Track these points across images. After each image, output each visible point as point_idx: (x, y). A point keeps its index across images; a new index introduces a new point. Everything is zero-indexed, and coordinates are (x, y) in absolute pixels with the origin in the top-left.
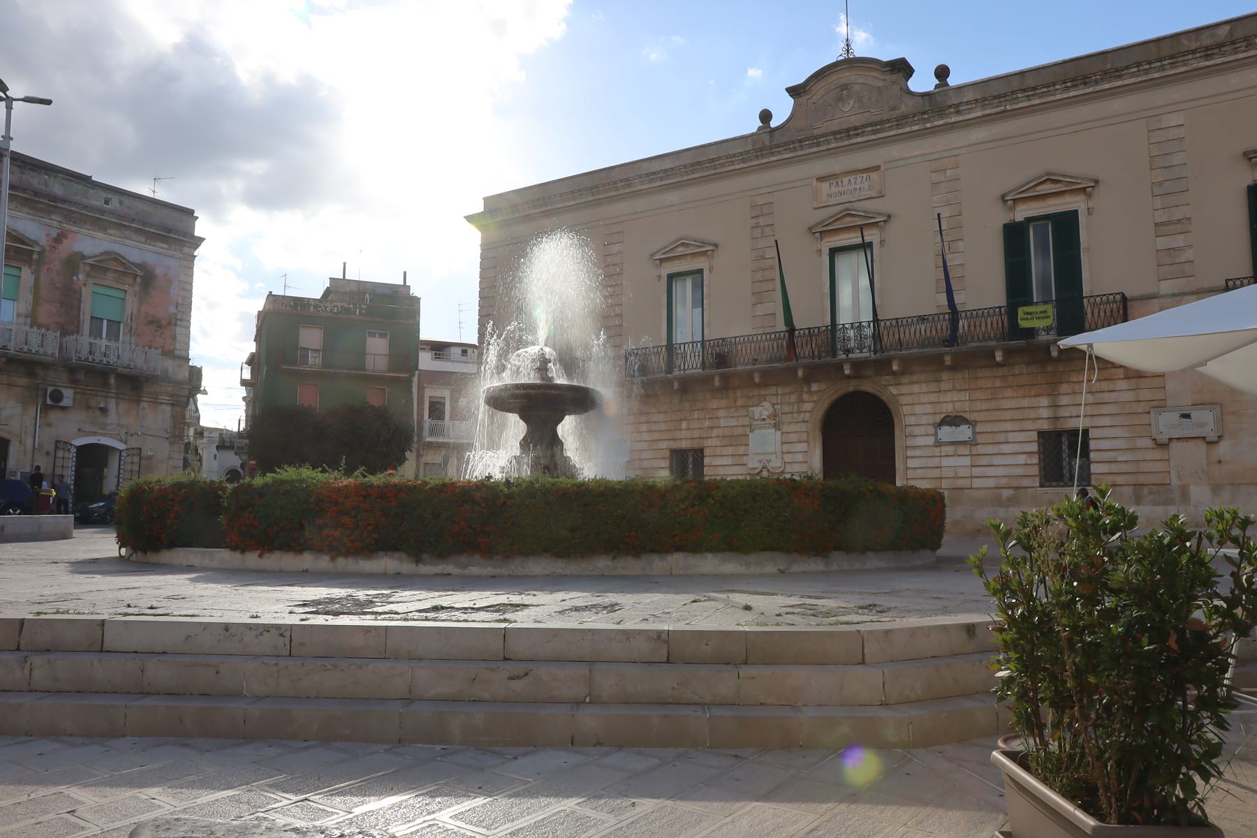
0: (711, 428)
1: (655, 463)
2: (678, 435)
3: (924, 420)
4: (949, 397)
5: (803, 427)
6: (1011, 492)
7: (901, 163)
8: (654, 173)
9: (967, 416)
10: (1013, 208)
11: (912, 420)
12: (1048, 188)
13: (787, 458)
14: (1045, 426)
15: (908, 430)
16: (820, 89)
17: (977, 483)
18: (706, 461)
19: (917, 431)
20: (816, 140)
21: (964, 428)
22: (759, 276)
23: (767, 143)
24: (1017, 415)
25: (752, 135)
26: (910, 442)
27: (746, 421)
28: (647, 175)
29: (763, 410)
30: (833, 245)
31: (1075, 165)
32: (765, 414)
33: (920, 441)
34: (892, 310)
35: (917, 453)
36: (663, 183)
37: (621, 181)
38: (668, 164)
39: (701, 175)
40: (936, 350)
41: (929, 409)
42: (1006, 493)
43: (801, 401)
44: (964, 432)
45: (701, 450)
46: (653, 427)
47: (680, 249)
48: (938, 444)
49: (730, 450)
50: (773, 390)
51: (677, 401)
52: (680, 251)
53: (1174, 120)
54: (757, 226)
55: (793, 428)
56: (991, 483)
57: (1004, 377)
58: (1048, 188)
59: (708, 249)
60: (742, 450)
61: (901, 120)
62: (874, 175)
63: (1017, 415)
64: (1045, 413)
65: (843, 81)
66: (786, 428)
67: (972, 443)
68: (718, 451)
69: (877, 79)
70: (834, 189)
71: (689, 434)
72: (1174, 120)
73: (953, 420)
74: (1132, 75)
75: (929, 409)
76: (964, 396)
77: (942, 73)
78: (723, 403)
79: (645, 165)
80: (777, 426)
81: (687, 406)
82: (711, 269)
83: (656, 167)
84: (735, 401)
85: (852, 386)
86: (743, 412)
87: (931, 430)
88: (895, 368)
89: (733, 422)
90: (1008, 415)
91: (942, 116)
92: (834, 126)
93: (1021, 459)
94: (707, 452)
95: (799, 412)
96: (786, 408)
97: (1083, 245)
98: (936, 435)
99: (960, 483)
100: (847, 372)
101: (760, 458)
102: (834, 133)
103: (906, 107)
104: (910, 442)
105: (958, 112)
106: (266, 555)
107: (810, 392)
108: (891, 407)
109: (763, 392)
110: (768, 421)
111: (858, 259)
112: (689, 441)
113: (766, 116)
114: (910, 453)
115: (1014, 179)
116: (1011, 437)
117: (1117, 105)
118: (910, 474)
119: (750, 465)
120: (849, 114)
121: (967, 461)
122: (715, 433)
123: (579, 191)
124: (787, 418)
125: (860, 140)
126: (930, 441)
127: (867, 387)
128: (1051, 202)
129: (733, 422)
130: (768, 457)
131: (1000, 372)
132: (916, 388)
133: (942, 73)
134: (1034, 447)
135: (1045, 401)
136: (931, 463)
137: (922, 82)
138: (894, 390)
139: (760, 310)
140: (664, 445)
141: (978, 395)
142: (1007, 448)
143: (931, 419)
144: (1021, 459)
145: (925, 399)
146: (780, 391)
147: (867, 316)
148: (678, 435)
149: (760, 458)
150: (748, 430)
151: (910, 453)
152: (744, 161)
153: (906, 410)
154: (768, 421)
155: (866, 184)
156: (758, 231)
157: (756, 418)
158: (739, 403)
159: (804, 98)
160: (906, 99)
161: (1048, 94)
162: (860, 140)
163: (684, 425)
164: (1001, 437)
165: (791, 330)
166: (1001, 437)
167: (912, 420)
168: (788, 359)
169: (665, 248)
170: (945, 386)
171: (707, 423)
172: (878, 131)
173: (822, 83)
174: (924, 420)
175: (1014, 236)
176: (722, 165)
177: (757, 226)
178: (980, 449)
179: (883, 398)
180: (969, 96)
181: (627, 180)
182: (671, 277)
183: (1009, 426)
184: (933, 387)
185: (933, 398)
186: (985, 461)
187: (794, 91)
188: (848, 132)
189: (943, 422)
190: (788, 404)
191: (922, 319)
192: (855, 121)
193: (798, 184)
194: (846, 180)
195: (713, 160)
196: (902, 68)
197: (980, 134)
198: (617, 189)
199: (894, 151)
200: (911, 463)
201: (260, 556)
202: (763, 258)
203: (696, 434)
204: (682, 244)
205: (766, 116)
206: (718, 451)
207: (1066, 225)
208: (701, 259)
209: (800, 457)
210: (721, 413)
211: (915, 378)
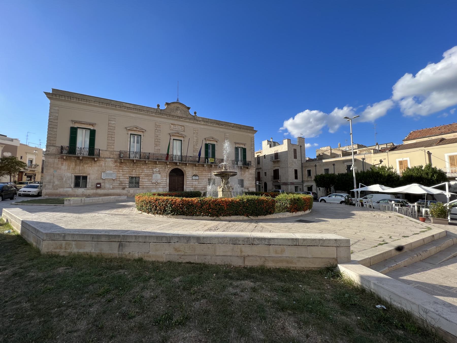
0: (142, 172)
1: (124, 180)
2: (132, 173)
3: (190, 175)
4: (195, 171)
5: (166, 174)
6: (204, 188)
7: (188, 127)
8: (130, 108)
9: (198, 175)
10: (206, 141)
11: (188, 175)
12: (211, 139)
13: (162, 180)
14: (209, 178)
15: (187, 177)
16: (173, 105)
17: (199, 187)
18: (140, 180)
19: (189, 177)
20: (173, 116)
21: (197, 177)
22: (156, 140)
23: (160, 112)
24: (205, 175)
25: (156, 109)
26: (187, 179)
27: (152, 172)
28: (127, 107)
29: (157, 169)
30: (174, 138)
31: (215, 137)
32: (157, 171)
33: (189, 179)
34: (184, 154)
35: (189, 181)
36: (131, 111)
37: (118, 106)
38: (131, 106)
39: (143, 113)
40: (196, 163)
41: (191, 173)
42: (203, 188)
43: (165, 168)
44: (197, 178)
45: (139, 177)
46: (124, 171)
47: (135, 128)
48: (192, 179)
49: (147, 178)
50: (159, 166)
51: (132, 165)
52: (135, 129)
53: (228, 135)
54: (157, 129)
55: (163, 174)
56: (201, 187)
57: (204, 169)
58: (211, 139)
59: (143, 131)
60: (150, 178)
61: (190, 119)
62: (183, 127)
63: (205, 175)
64: (210, 176)
65: (177, 106)
66: (161, 174)
67: (198, 180)
68: (144, 178)
69: (185, 109)
70: (174, 127)
71: (135, 173)
72: (228, 135)
73: (195, 175)
74: (224, 126)
75: (191, 173)
76: (197, 171)
77: (195, 113)
78: (146, 167)
79: (124, 104)
80: (160, 173)
81: (135, 166)
82: (144, 136)
83: (128, 106)
84: (149, 167)
85: (176, 167)
86: (151, 170)
87: (191, 177)
88: (188, 165)
89: (148, 172)
90: (204, 175)
91: (197, 121)
92: (175, 114)
93: (206, 183)
94: (140, 178)
95: (165, 171)
96: (162, 170)
97: (216, 150)
98: (192, 178)
99: (196, 186)
100: (178, 164)
101: (156, 180)
102: (177, 116)
103: (189, 117)
104: (187, 179)
105: (200, 122)
106: (297, 213)
107: (167, 167)
108: (184, 172)
109: (156, 166)
110: (158, 172)
111: (179, 142)
112: (135, 175)
113: (158, 106)
114: (187, 181)
115: (207, 136)
116: (204, 179)
117: (221, 130)
118: (187, 185)
119: (153, 181)
120: (178, 113)
121: (197, 183)
122: (143, 174)
123: (102, 103)
124: (162, 172)
125: (182, 120)
126: (191, 179)
127: (179, 168)
128: (212, 142)
129: (148, 172)
130: (158, 180)
131: (203, 168)
132: (189, 169)
133: (195, 113)
134: (207, 181)
135: (209, 174)
136: (191, 183)
137: (191, 112)
138: (185, 169)
139: (156, 148)
140: (128, 175)
141: (199, 171)
142: (203, 181)
143: (191, 175)
144: (206, 183)
145: (190, 171)
146: (160, 166)
147: (179, 154)
148: (132, 173)
149: (156, 180)
150: (152, 174)
151: (187, 181)
152: (155, 114)
153: (187, 173)
154: (158, 172)
155: (181, 128)
156: (157, 130)
157: (155, 171)
158: (150, 167)
159: (169, 106)
160: (190, 115)
161: (213, 124)
162: (182, 120)
163: (134, 171)
164: (203, 179)
165: (168, 154)
166: (203, 179)
167: (188, 175)
168: (166, 160)
169: (131, 127)
170: (194, 169)
171: (141, 171)
172: (186, 119)
173: (173, 105)
174: (190, 175)
175: (207, 146)
176: (150, 113)
177: (157, 129)
178: (199, 181)
179: (182, 170)
180: (200, 119)
181: (121, 106)
182: (131, 134)
183: (204, 177)
184: (192, 169)
185: (192, 171)
186: (200, 183)
187: (167, 104)
188: (180, 117)
189: (193, 176)
190: (163, 169)
191: (190, 156)
192: (180, 115)
193: (167, 123)
194: (177, 126)
195: (148, 111)
196: (189, 108)
197: (202, 127)
198: (116, 107)
199: (187, 124)
200: (187, 183)
201: (296, 213)
202: (158, 137)
203: (137, 173)
204: (135, 128)
205: (158, 106)
206: (144, 178)
207: (213, 146)
208: (141, 132)
209: (165, 180)
210: (145, 169)
211: (189, 167)
